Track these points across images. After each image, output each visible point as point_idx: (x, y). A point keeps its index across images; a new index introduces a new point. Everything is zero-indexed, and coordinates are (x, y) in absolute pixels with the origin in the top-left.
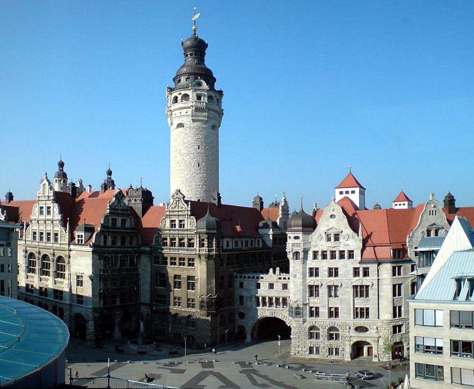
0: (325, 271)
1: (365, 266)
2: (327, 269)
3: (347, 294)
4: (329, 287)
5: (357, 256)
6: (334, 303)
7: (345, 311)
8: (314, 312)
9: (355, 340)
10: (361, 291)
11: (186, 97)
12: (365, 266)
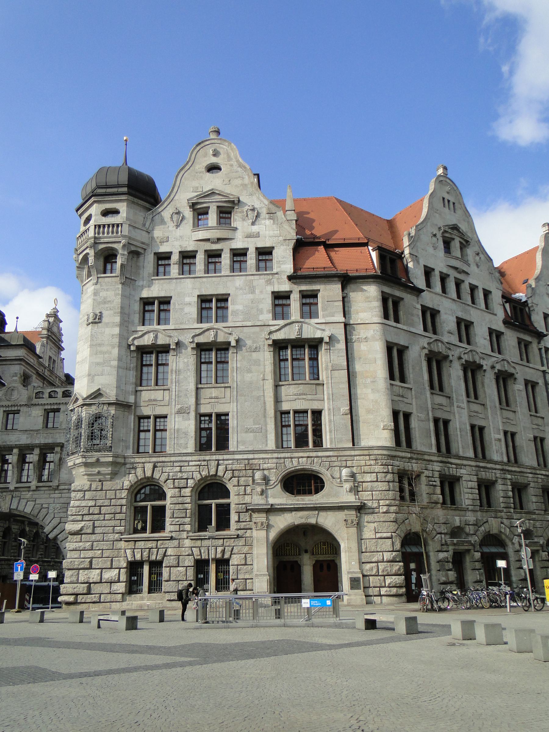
2: (195, 299)
3: (253, 368)
4: (202, 348)
5: (283, 261)
6: (215, 401)
7: (250, 423)
9: (282, 522)
10: (296, 353)
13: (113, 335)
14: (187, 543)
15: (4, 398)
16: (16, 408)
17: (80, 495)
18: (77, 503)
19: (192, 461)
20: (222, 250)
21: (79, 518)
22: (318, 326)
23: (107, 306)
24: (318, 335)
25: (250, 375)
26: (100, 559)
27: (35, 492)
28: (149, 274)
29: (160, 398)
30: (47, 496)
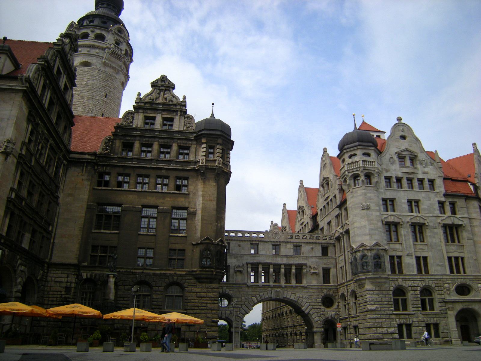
0: (404, 203)
1: (451, 200)
2: (406, 201)
4: (414, 225)
8: (397, 264)
11: (100, 37)
12: (451, 200)
13: (377, 216)
14: (421, 316)
15: (271, 237)
16: (278, 243)
17: (371, 292)
18: (371, 296)
19: (417, 278)
20: (413, 178)
21: (373, 303)
22: (460, 219)
23: (371, 201)
24: (460, 223)
25: (435, 239)
26: (385, 323)
27: (295, 289)
28: (384, 186)
29: (398, 248)
30: (301, 291)
